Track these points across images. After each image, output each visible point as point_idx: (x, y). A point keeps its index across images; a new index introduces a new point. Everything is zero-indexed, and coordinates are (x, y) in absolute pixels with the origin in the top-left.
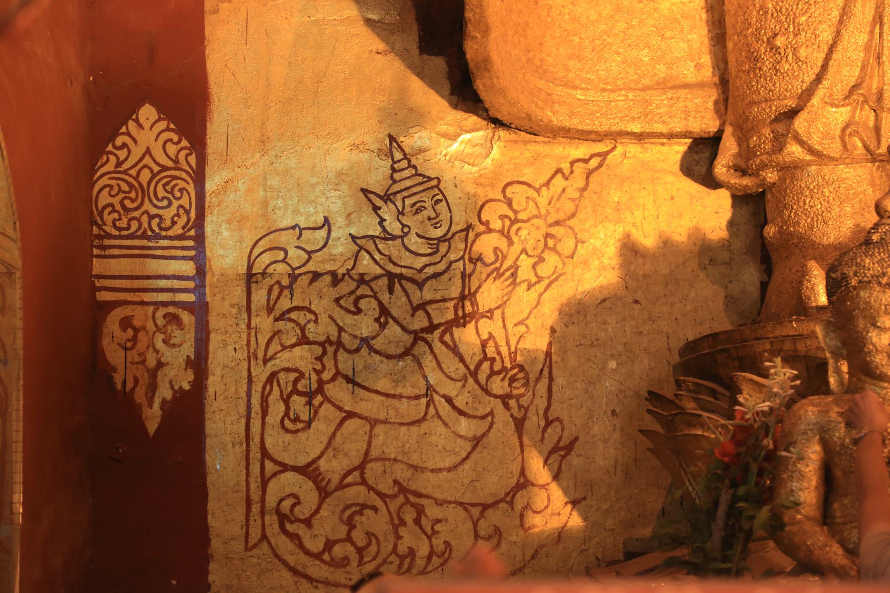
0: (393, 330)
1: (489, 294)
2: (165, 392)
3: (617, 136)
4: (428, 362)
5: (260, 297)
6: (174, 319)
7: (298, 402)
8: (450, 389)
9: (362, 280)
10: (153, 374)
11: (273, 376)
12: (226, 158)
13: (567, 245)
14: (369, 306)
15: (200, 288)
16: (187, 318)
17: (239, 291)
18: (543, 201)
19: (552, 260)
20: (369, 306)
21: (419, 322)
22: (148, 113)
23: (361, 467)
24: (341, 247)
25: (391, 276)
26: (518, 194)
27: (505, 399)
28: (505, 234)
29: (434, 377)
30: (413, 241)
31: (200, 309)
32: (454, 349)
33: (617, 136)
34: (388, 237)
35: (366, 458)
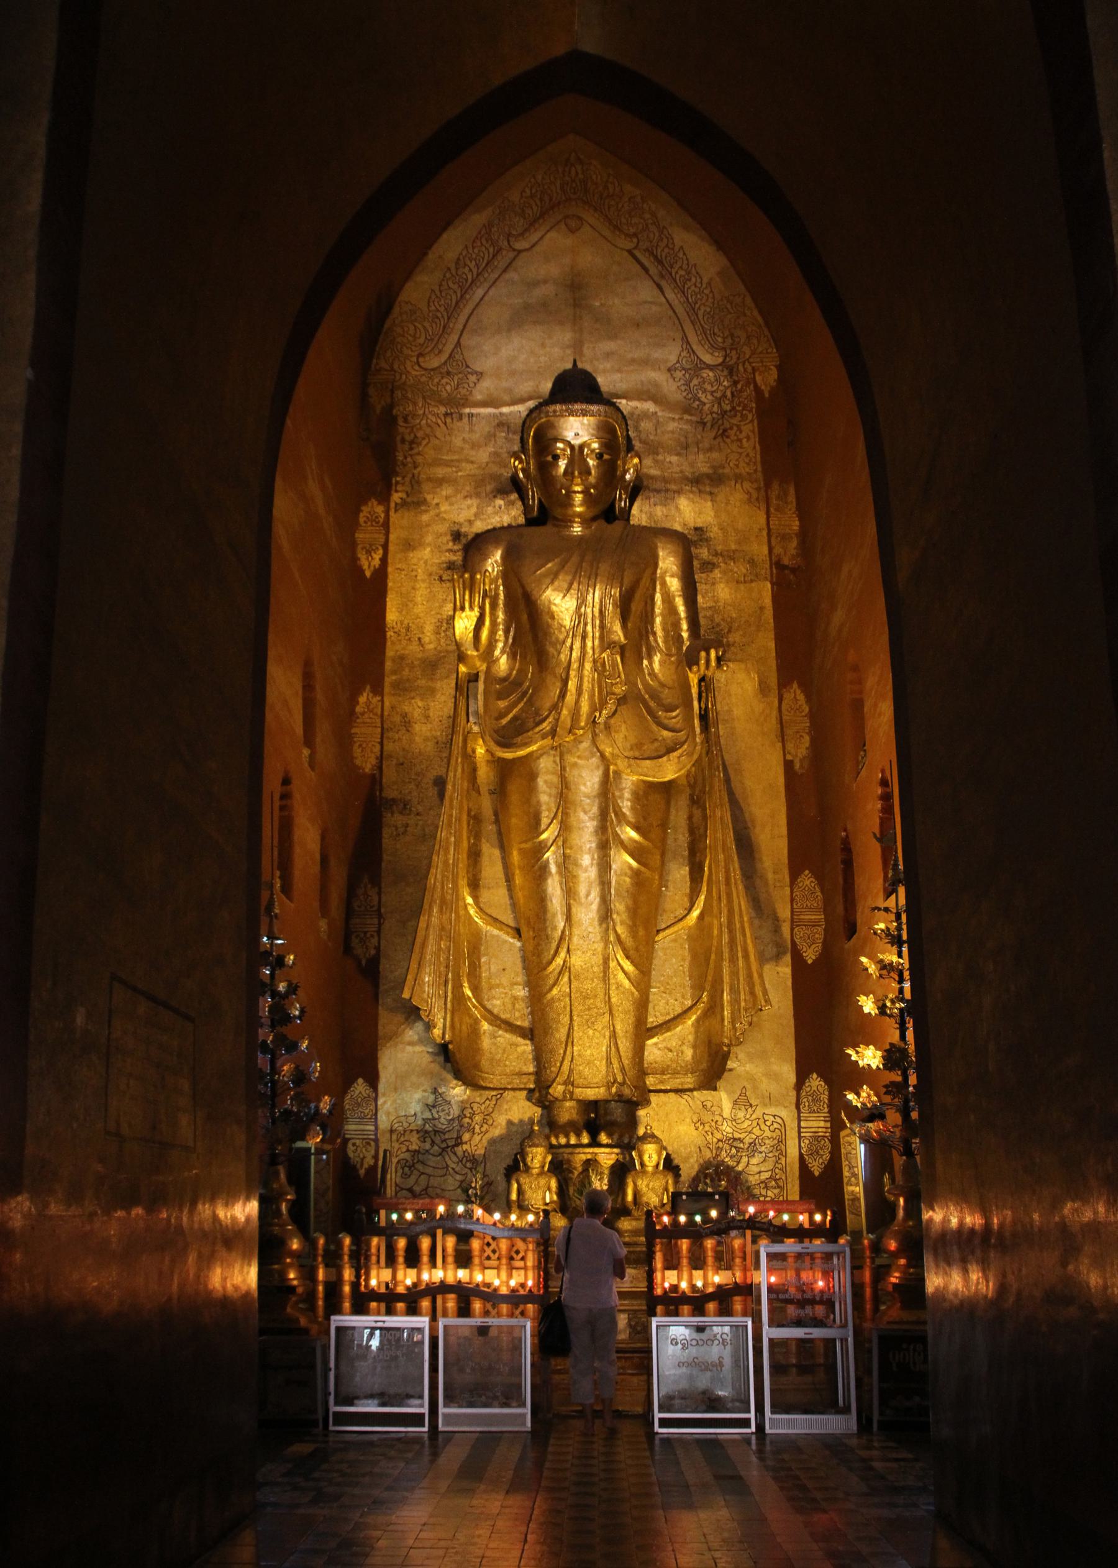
0: (436, 1147)
1: (466, 1137)
2: (366, 1166)
3: (505, 1089)
4: (447, 1158)
5: (394, 1137)
6: (369, 1144)
7: (406, 1169)
8: (454, 1166)
9: (426, 1132)
10: (362, 1159)
11: (399, 1162)
12: (384, 1095)
13: (490, 1122)
14: (428, 1140)
15: (376, 1135)
16: (372, 1143)
17: (388, 1135)
18: (483, 1108)
19: (485, 1126)
20: (428, 1140)
21: (444, 1145)
22: (360, 1081)
23: (426, 1189)
24: (420, 1122)
25: (436, 1132)
26: (475, 1106)
27: (471, 1169)
28: (471, 1118)
29: (449, 1163)
30: (442, 1120)
31: (376, 1141)
32: (455, 1154)
33: (505, 1089)
34: (434, 1119)
35: (428, 1187)
